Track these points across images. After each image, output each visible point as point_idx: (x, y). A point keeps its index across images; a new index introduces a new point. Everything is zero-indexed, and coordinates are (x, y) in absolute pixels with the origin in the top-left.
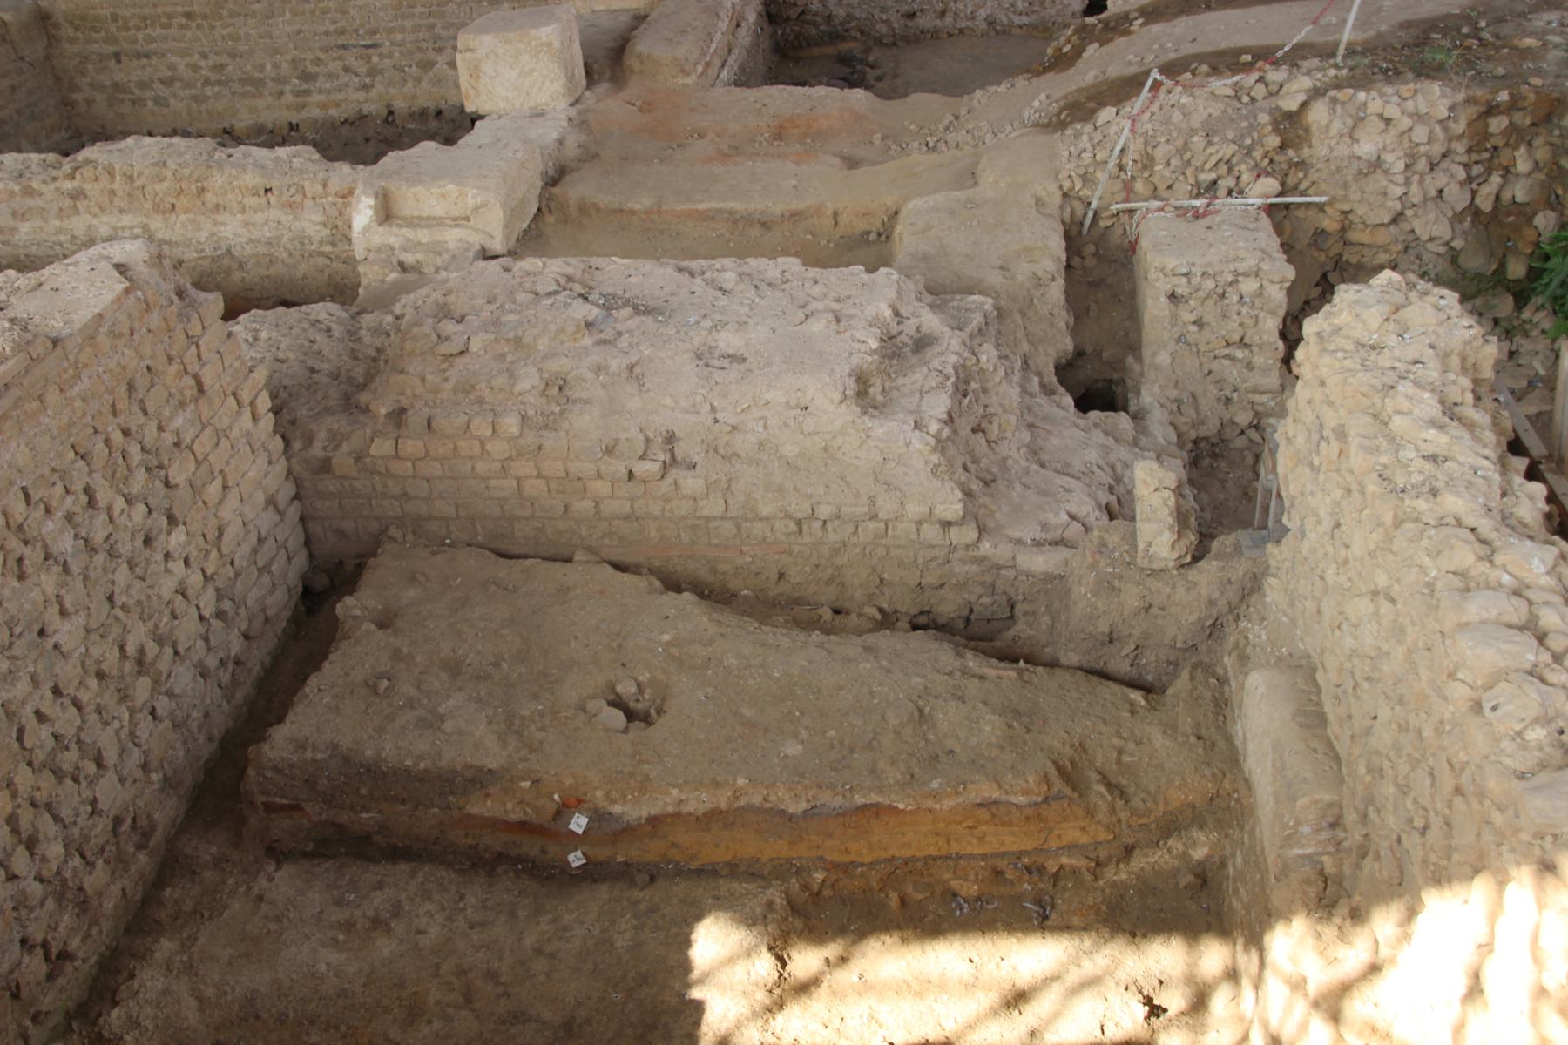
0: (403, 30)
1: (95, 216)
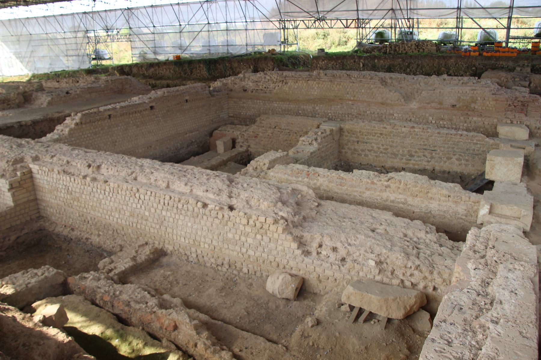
0: (444, 147)
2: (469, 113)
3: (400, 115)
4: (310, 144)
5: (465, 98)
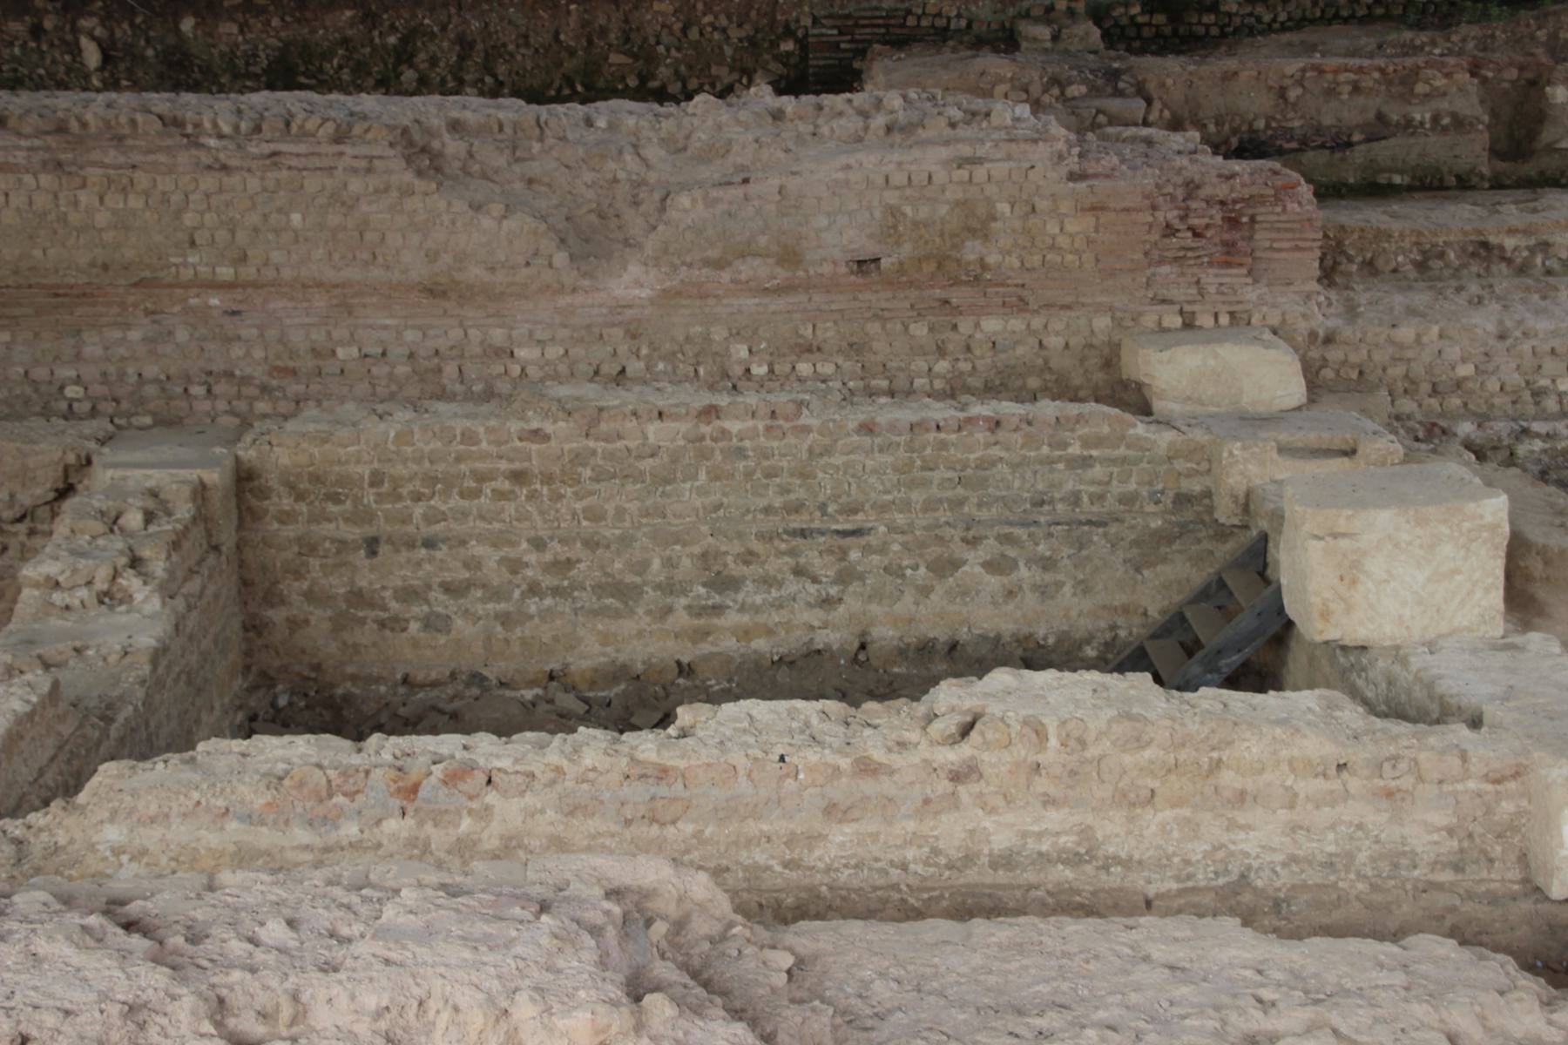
0: (906, 506)
1: (993, 811)
2: (957, 296)
3: (554, 352)
4: (106, 598)
5: (924, 212)
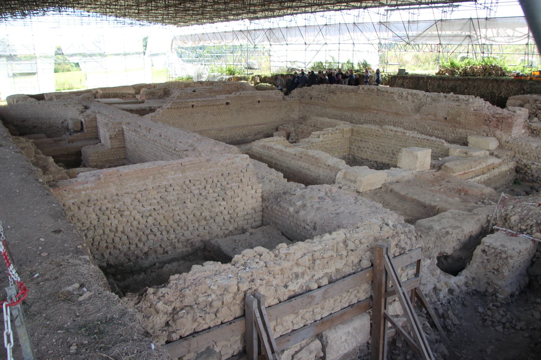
2: (456, 125)
3: (408, 124)
5: (453, 112)
